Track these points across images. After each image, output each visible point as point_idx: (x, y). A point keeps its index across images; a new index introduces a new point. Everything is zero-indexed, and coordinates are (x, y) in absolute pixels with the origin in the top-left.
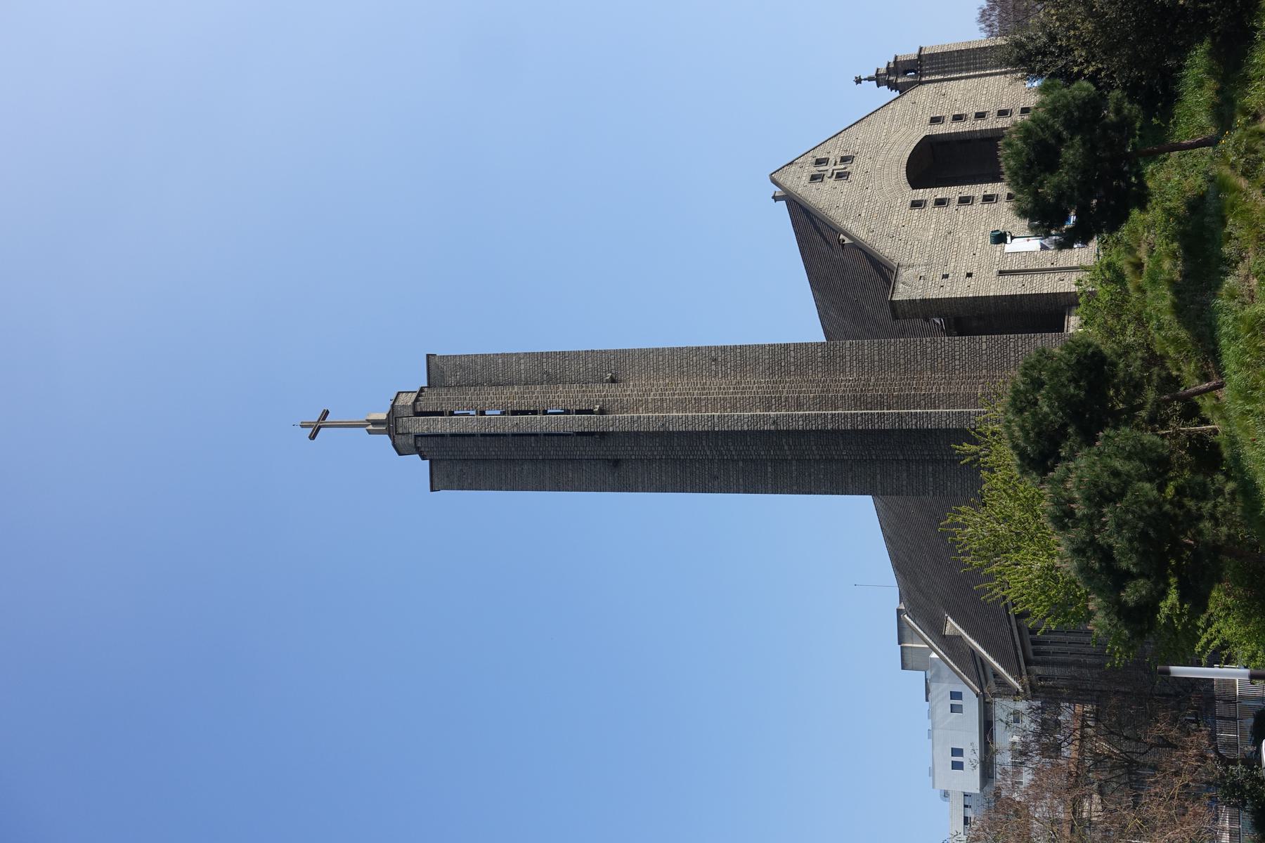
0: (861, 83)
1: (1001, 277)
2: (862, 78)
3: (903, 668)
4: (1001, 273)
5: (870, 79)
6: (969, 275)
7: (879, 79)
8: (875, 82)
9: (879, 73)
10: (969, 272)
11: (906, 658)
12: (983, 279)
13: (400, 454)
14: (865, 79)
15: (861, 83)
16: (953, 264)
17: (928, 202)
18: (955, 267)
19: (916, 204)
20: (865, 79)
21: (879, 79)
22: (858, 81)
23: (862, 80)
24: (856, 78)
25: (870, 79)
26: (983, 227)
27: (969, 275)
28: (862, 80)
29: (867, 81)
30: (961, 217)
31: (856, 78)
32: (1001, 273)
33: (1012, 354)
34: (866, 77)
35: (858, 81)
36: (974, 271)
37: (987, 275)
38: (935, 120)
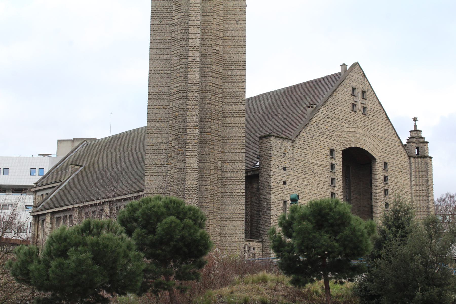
0: (413, 121)
1: (282, 202)
2: (416, 122)
3: (59, 141)
5: (415, 126)
6: (285, 183)
8: (413, 129)
10: (287, 183)
11: (65, 142)
12: (282, 191)
14: (415, 123)
15: (413, 121)
16: (292, 173)
17: (333, 160)
18: (290, 175)
20: (415, 123)
22: (415, 119)
24: (417, 118)
25: (415, 126)
26: (315, 192)
27: (285, 183)
30: (323, 180)
33: (233, 208)
34: (417, 125)
35: (415, 119)
37: (284, 194)
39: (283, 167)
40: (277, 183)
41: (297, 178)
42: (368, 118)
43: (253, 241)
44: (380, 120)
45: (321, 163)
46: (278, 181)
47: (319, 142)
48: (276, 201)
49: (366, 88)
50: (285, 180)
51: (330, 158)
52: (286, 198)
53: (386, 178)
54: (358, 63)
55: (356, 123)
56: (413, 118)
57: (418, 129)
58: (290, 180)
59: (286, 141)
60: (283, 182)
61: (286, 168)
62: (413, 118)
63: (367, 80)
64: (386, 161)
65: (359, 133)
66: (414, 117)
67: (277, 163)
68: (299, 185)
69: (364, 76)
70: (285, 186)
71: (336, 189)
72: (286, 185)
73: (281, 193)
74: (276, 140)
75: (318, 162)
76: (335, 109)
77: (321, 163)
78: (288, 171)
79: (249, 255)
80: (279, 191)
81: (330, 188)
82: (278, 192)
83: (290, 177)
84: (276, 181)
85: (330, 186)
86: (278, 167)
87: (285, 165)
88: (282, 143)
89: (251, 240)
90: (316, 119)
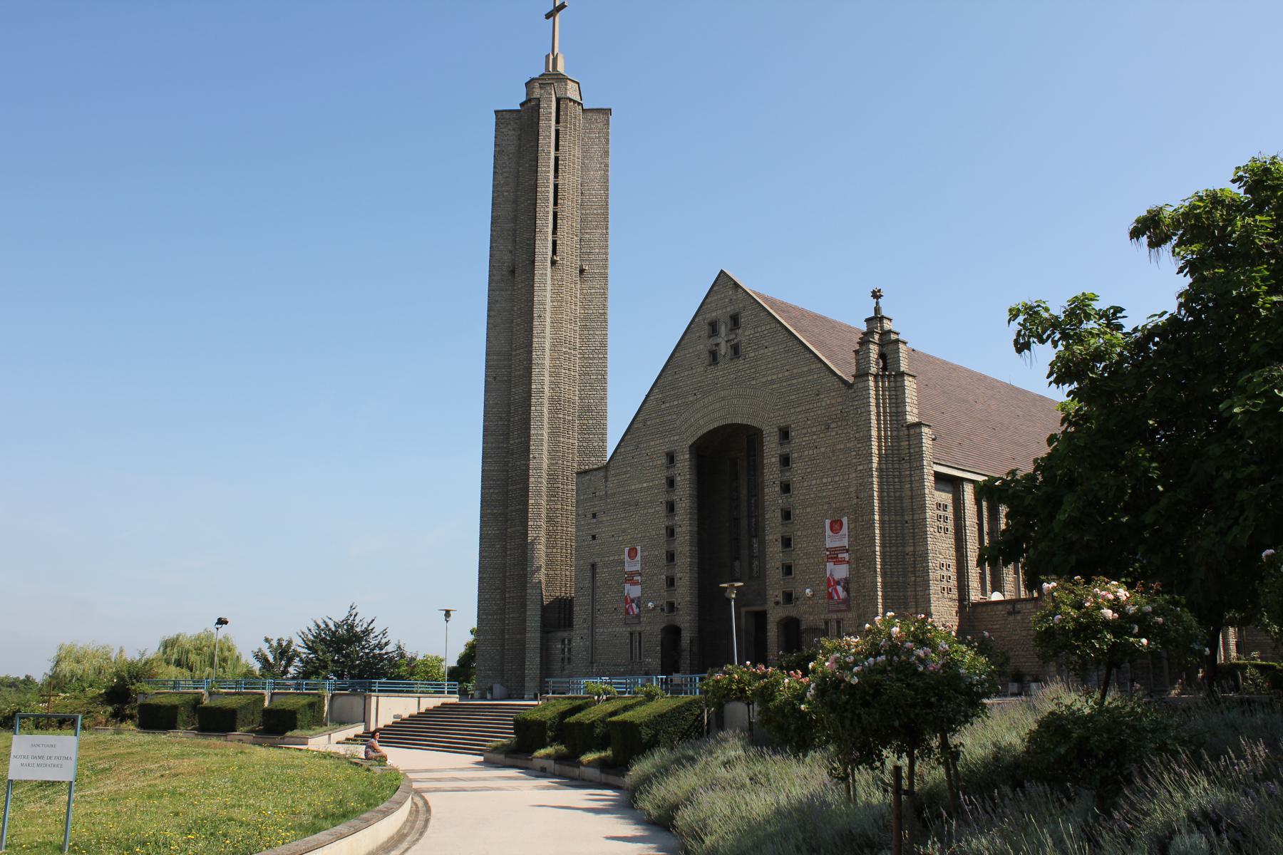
4: (593, 566)
5: (877, 310)
6: (594, 537)
9: (885, 321)
13: (526, 84)
14: (877, 303)
16: (604, 519)
17: (673, 469)
19: (671, 458)
20: (877, 303)
22: (876, 295)
24: (879, 291)
25: (877, 310)
27: (594, 537)
31: (879, 291)
32: (593, 566)
35: (876, 295)
36: (598, 541)
38: (785, 434)
53: (785, 461)
69: (736, 286)
75: (645, 485)
86: (585, 516)
88: (590, 480)
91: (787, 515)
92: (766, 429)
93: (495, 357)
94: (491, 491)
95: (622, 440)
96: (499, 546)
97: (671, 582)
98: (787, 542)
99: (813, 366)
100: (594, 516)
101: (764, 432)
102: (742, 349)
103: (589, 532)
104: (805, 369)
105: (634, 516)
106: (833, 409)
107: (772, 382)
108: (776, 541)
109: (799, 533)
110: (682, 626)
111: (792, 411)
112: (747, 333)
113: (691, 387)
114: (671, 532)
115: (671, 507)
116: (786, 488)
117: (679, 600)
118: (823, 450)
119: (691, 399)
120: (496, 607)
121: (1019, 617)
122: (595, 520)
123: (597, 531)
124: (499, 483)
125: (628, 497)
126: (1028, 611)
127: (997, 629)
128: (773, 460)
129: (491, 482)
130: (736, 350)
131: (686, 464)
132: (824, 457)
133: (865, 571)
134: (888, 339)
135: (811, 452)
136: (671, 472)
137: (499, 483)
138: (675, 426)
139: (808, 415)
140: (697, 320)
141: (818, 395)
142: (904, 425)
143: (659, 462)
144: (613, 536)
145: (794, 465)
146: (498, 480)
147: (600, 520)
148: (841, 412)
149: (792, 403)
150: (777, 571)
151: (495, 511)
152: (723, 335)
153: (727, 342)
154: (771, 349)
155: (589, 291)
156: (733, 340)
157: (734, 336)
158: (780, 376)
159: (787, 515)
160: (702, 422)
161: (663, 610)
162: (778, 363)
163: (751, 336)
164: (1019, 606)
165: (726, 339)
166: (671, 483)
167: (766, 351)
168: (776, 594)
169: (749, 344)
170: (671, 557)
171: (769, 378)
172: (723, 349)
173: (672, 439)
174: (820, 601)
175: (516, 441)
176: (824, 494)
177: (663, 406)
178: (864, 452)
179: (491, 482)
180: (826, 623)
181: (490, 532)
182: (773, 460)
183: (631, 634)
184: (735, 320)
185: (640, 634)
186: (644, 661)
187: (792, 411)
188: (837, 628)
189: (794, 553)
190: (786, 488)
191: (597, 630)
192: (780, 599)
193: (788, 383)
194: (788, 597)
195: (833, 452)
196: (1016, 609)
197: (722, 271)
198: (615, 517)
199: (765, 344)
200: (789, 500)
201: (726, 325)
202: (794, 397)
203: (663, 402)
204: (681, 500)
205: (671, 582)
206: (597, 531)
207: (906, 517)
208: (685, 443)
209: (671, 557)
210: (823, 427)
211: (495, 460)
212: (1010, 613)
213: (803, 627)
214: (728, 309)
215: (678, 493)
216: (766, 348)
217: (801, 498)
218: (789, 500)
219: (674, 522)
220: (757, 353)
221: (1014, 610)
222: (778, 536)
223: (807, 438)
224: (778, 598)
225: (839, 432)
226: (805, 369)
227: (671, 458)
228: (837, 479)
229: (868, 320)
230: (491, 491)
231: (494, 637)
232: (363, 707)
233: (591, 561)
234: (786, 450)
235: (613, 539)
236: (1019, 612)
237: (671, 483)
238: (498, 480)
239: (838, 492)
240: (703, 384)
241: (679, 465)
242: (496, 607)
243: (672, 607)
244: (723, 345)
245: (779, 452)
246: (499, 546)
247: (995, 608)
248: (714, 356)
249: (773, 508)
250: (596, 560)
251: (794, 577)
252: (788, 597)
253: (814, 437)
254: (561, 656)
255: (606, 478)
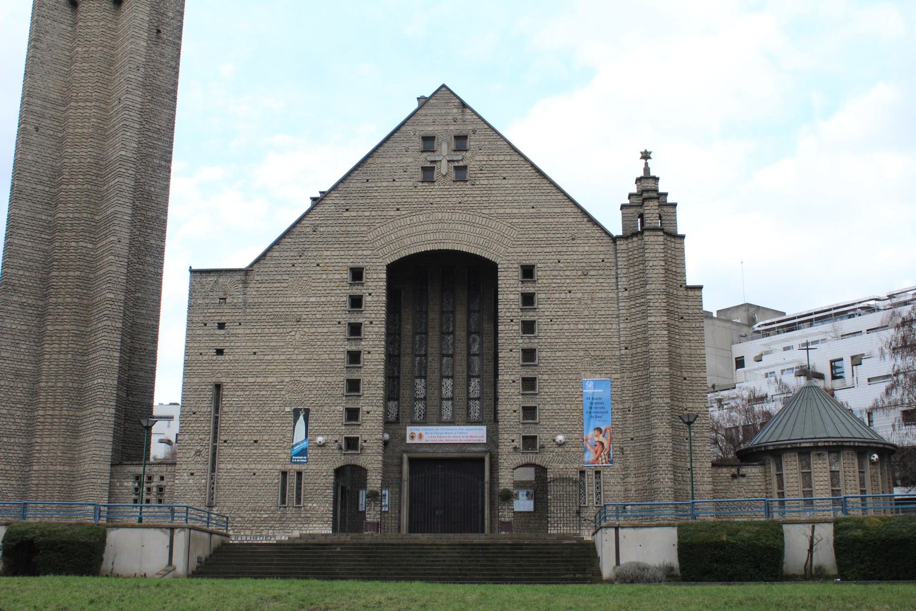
0: (642, 158)
2: (648, 161)
5: (647, 169)
7: (647, 181)
10: (225, 351)
14: (646, 164)
15: (642, 158)
16: (238, 331)
17: (359, 287)
18: (235, 335)
19: (357, 274)
20: (646, 164)
21: (647, 181)
22: (646, 156)
23: (646, 160)
25: (647, 169)
28: (646, 160)
29: (644, 166)
30: (325, 330)
32: (218, 387)
34: (649, 166)
35: (646, 156)
38: (528, 272)
39: (218, 323)
40: (201, 354)
41: (253, 338)
42: (472, 187)
43: (139, 464)
44: (510, 182)
45: (323, 299)
46: (201, 351)
47: (319, 261)
48: (194, 387)
49: (469, 128)
50: (220, 346)
51: (349, 285)
52: (223, 378)
53: (528, 300)
54: (444, 86)
55: (431, 204)
56: (642, 153)
57: (652, 174)
58: (232, 344)
59: (228, 274)
60: (215, 351)
61: (225, 323)
62: (642, 153)
63: (473, 111)
64: (531, 261)
65: (441, 221)
66: (643, 150)
67: (201, 318)
68: (257, 350)
69: (464, 105)
70: (220, 357)
71: (363, 343)
72: (222, 355)
73: (209, 371)
74: (201, 278)
76: (368, 189)
77: (323, 299)
78: (230, 329)
79: (149, 489)
80: (203, 368)
81: (346, 343)
82: (201, 371)
83: (233, 338)
84: (196, 351)
85: (348, 339)
86: (205, 325)
87: (223, 318)
89: (129, 463)
90: (313, 219)
91: (529, 355)
92: (502, 264)
93: (39, 102)
94: (21, 272)
95: (277, 242)
96: (25, 347)
97: (352, 414)
98: (529, 384)
99: (569, 210)
100: (221, 326)
101: (499, 266)
102: (469, 174)
103: (214, 345)
104: (558, 210)
105: (293, 333)
106: (593, 257)
107: (511, 216)
108: (514, 382)
109: (545, 377)
110: (369, 467)
111: (539, 250)
112: (477, 158)
113: (392, 200)
114: (354, 357)
115: (355, 330)
116: (528, 327)
117: (365, 437)
118: (579, 295)
119: (392, 213)
120: (14, 427)
121: (744, 480)
122: (222, 332)
123: (228, 344)
124: (31, 264)
125: (283, 310)
126: (754, 475)
127: (721, 489)
128: (512, 297)
129: (22, 262)
130: (461, 171)
131: (381, 284)
132: (580, 303)
133: (656, 421)
134: (663, 200)
135: (563, 296)
136: (356, 291)
137: (31, 264)
138: (366, 239)
139: (560, 257)
140: (403, 129)
141: (573, 239)
142: (684, 286)
143: (337, 276)
144: (255, 353)
145: (540, 306)
146: (30, 260)
147: (231, 332)
148: (603, 261)
149: (539, 242)
150: (515, 414)
151: (24, 300)
152: (445, 153)
153: (449, 161)
154: (510, 182)
155: (159, 58)
156: (458, 161)
157: (460, 158)
158: (523, 211)
159: (529, 355)
160: (407, 241)
161: (340, 448)
162: (521, 198)
163: (485, 163)
164: (744, 470)
165: (448, 159)
166: (356, 302)
167: (504, 182)
168: (512, 438)
169: (481, 170)
170: (353, 386)
171: (508, 211)
172: (444, 167)
173: (360, 253)
174: (573, 449)
175: (71, 215)
176: (580, 340)
177: (346, 214)
178: (657, 304)
179: (22, 262)
180: (582, 473)
181: (14, 327)
182: (512, 297)
183: (284, 474)
184: (461, 140)
185: (299, 474)
186: (304, 506)
187: (539, 250)
188: (297, 493)
189: (538, 397)
190: (528, 327)
191: (222, 466)
192: (519, 443)
193: (535, 220)
194: (530, 442)
195: (592, 299)
196: (741, 473)
197: (444, 86)
198: (259, 331)
199: (504, 175)
200: (532, 341)
201: (449, 145)
202: (541, 236)
203: (347, 210)
204: (371, 323)
205: (352, 414)
206: (228, 344)
207: (684, 373)
208: (380, 260)
209: (353, 386)
210: (580, 273)
211: (29, 233)
212: (734, 476)
213: (550, 476)
214: (452, 128)
215: (368, 315)
216: (504, 178)
217: (549, 340)
218: (532, 341)
219: (360, 348)
220: (491, 182)
221: (738, 473)
222: (518, 377)
223: (559, 281)
224: (515, 443)
225: (601, 281)
226: (558, 210)
227: (357, 274)
228: (597, 327)
229: (639, 180)
230: (21, 272)
231: (8, 468)
232: (168, 543)
233: (214, 380)
234: (529, 288)
235: (255, 357)
236: (743, 476)
237: (356, 302)
238: (30, 260)
239: (598, 340)
240: (412, 200)
241: (370, 284)
242: (14, 427)
243: (352, 443)
244: (444, 162)
245: (520, 289)
246: (25, 347)
247: (719, 470)
248: (428, 172)
249: (510, 347)
250: (223, 380)
251: (539, 422)
252: (530, 442)
253: (568, 281)
254: (134, 496)
255: (245, 282)
